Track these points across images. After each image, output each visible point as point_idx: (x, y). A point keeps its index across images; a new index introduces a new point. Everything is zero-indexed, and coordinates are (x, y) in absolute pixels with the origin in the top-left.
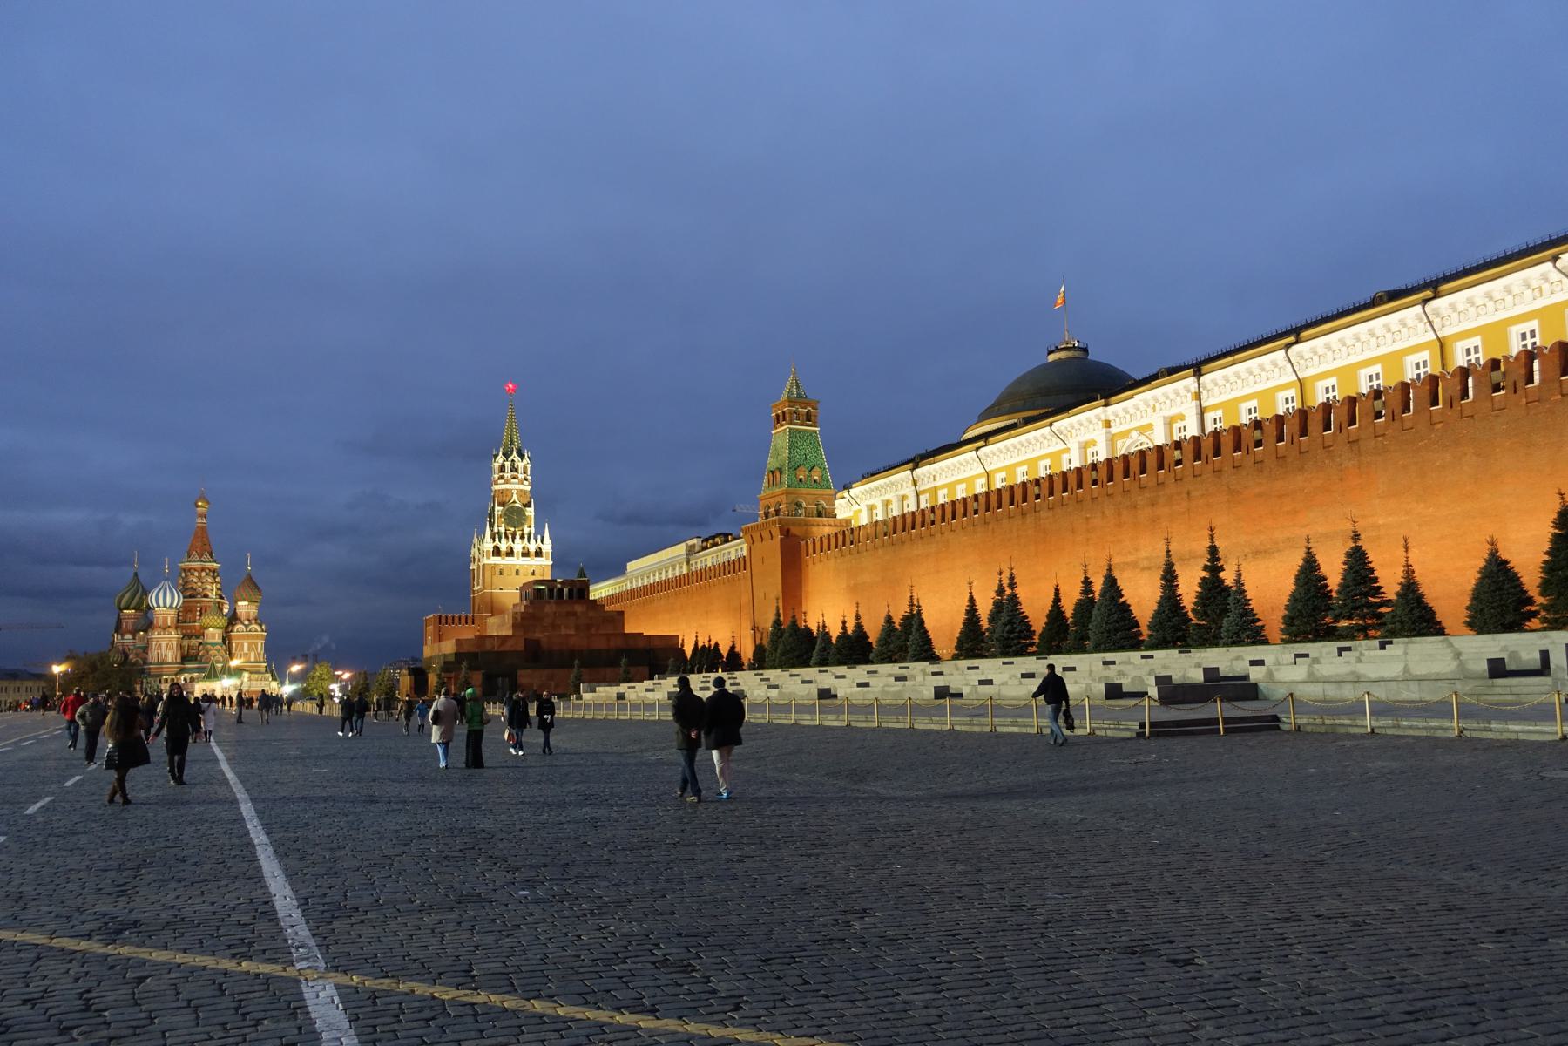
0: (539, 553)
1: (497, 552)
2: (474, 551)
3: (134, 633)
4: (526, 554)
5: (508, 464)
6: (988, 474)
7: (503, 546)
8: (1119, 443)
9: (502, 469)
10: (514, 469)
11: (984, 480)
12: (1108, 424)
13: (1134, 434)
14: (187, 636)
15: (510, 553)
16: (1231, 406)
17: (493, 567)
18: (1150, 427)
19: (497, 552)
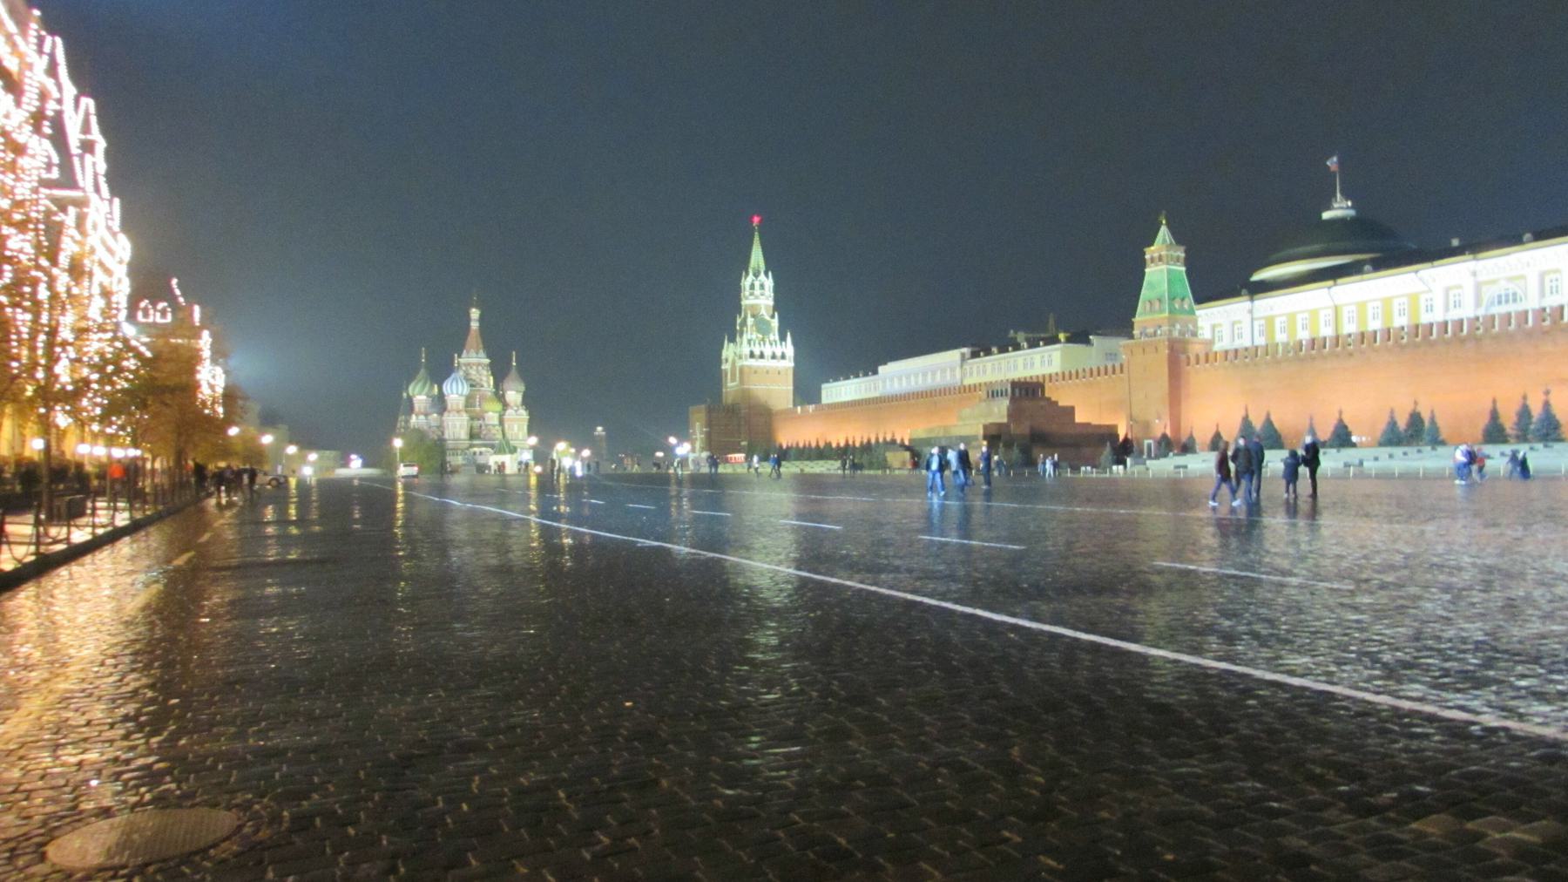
0: (783, 357)
1: (752, 355)
3: (426, 415)
4: (774, 357)
6: (1336, 309)
7: (757, 353)
8: (1484, 289)
9: (752, 287)
10: (762, 286)
11: (1330, 312)
12: (1474, 274)
14: (472, 419)
15: (762, 356)
17: (750, 367)
18: (1523, 277)
19: (752, 355)
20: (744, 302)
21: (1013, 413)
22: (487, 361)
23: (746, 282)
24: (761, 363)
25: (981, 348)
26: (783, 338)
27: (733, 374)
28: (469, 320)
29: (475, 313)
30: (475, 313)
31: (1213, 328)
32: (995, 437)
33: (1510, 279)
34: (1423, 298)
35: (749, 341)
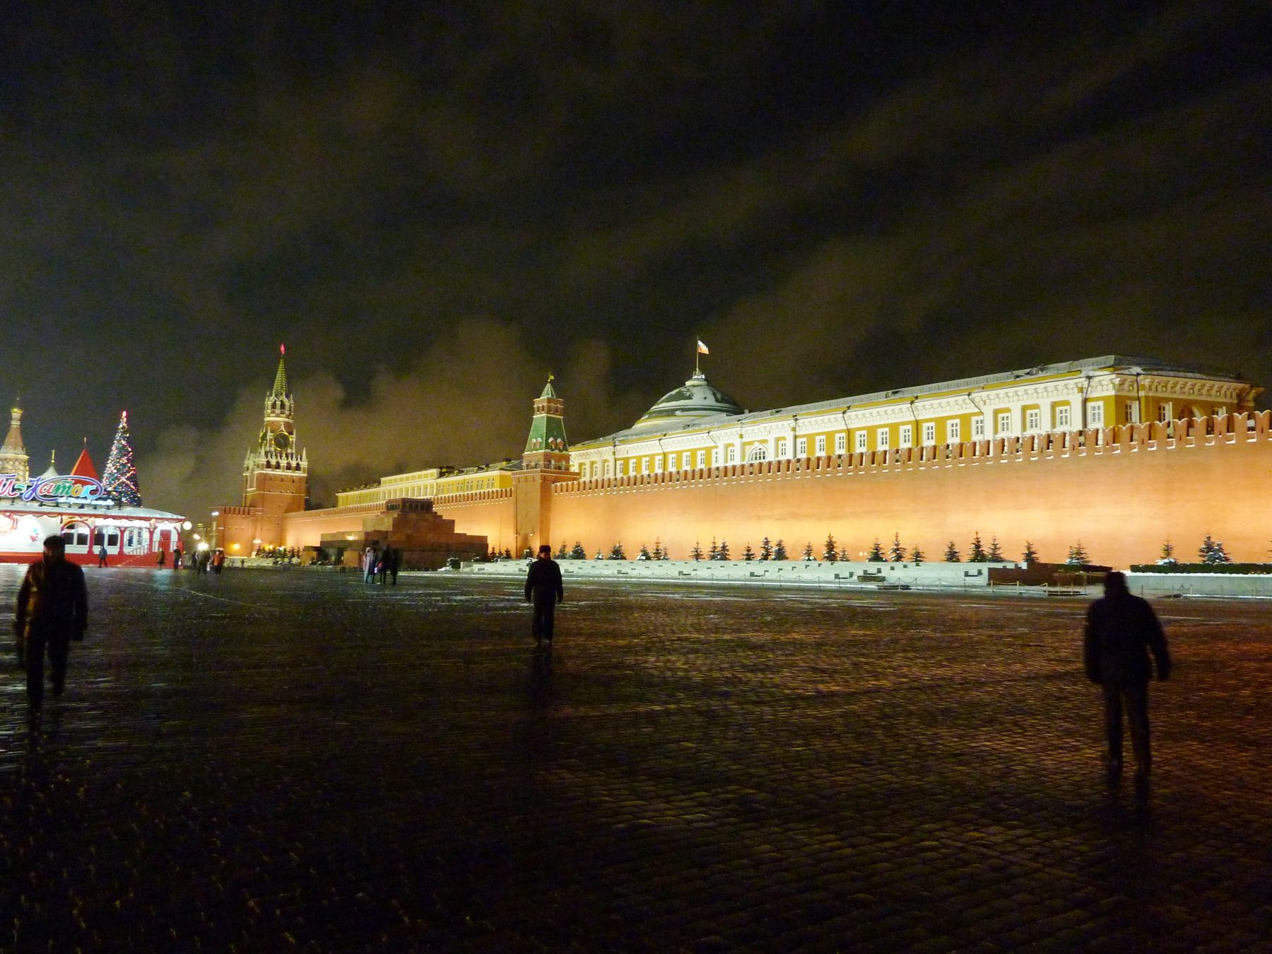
0: (298, 468)
2: (249, 462)
4: (289, 467)
5: (278, 403)
6: (665, 455)
7: (273, 462)
9: (274, 406)
10: (283, 406)
12: (741, 436)
13: (756, 444)
15: (278, 466)
16: (811, 438)
18: (766, 441)
19: (269, 465)
20: (267, 419)
21: (396, 524)
22: (26, 457)
23: (269, 403)
24: (278, 472)
25: (447, 469)
26: (299, 452)
27: (252, 481)
28: (9, 418)
29: (16, 413)
30: (16, 413)
31: (581, 465)
32: (373, 541)
33: (762, 442)
34: (714, 451)
35: (266, 454)
